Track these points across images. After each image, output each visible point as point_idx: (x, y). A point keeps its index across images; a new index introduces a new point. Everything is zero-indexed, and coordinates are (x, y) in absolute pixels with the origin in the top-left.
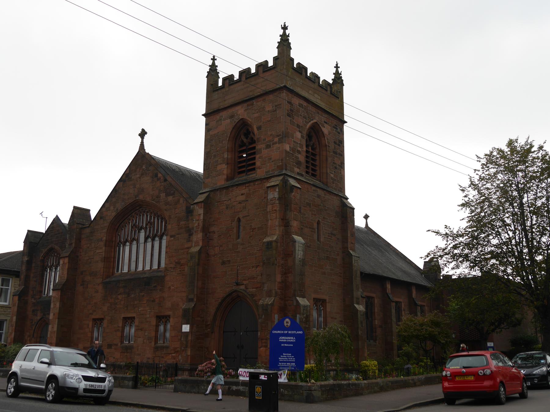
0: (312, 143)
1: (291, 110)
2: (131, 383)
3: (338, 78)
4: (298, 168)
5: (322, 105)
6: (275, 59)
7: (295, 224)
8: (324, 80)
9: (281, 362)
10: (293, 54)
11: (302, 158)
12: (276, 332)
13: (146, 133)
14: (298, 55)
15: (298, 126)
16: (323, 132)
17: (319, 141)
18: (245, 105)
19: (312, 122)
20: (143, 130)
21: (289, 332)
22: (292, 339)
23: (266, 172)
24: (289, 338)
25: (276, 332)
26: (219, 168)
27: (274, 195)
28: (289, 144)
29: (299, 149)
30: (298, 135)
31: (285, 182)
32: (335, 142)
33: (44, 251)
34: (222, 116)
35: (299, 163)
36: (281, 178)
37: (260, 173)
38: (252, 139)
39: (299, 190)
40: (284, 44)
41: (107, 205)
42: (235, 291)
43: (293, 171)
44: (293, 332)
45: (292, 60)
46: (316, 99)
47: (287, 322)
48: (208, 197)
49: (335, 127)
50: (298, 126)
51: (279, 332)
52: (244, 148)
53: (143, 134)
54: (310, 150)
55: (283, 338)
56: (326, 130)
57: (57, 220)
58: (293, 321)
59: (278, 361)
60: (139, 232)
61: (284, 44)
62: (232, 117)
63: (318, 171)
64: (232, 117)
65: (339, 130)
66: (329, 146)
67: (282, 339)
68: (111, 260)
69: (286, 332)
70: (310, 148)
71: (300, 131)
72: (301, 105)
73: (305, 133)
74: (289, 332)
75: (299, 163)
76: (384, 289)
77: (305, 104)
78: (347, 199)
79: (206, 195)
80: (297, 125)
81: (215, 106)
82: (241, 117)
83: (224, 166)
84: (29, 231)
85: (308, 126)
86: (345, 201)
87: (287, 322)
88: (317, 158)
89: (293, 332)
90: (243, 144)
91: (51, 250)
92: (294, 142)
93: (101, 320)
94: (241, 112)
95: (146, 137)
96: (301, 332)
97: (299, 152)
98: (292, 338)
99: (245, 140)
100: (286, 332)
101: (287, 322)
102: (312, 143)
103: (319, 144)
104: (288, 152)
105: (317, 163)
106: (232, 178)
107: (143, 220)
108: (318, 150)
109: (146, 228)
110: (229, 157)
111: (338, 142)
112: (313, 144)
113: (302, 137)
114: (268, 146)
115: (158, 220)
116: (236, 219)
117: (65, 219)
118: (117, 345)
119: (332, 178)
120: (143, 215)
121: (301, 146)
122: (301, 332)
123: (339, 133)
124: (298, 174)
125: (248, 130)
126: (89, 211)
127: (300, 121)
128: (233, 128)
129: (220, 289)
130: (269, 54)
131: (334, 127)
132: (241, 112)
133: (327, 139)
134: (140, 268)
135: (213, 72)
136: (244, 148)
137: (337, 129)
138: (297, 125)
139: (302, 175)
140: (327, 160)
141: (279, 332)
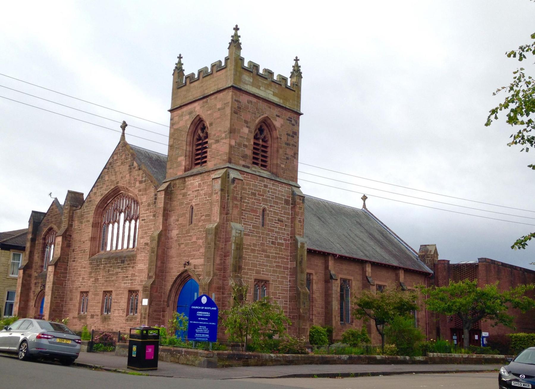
0: (262, 136)
1: (239, 108)
2: (86, 347)
3: (297, 72)
4: (244, 161)
5: (276, 100)
6: (227, 59)
7: (235, 212)
8: (279, 75)
9: (198, 333)
10: (243, 54)
11: (249, 152)
12: (194, 307)
13: (126, 125)
14: (248, 55)
15: (246, 122)
16: (274, 126)
17: (271, 134)
18: (201, 102)
19: (263, 116)
20: (124, 122)
21: (206, 308)
22: (207, 314)
23: (215, 165)
24: (205, 313)
25: (194, 307)
26: (180, 159)
27: (218, 185)
28: (234, 139)
29: (246, 143)
30: (246, 130)
31: (227, 175)
32: (287, 134)
33: (45, 230)
34: (183, 112)
35: (245, 157)
36: (223, 171)
37: (210, 165)
38: (207, 133)
39: (240, 182)
40: (235, 43)
41: (95, 190)
42: (186, 271)
43: (238, 164)
44: (209, 308)
45: (242, 60)
46: (269, 94)
47: (204, 300)
48: (168, 187)
49: (290, 120)
50: (246, 122)
51: (197, 307)
52: (200, 142)
53: (124, 126)
54: (261, 142)
55: (200, 313)
56: (278, 123)
57: (56, 202)
58: (209, 299)
59: (195, 333)
60: (119, 215)
61: (235, 43)
62: (190, 113)
63: (269, 162)
64: (190, 113)
65: (293, 122)
66: (281, 139)
67: (199, 313)
68: (99, 239)
69: (203, 308)
70: (261, 140)
71: (247, 127)
72: (249, 102)
73: (253, 128)
74: (206, 308)
75: (245, 157)
76: (364, 272)
77: (254, 100)
78: (299, 187)
79: (167, 184)
80: (245, 121)
81: (179, 103)
82: (198, 114)
83: (183, 158)
84: (33, 212)
85: (257, 121)
86: (295, 189)
87: (204, 300)
88: (269, 150)
89: (209, 308)
90: (199, 139)
91: (51, 229)
92: (241, 137)
93: (87, 292)
94: (197, 108)
95: (127, 128)
96: (215, 309)
97: (245, 146)
98: (207, 313)
99: (201, 135)
100: (203, 308)
101: (204, 300)
102: (262, 136)
103: (271, 137)
104: (234, 147)
105: (268, 154)
106: (191, 169)
107: (124, 203)
108: (269, 142)
109: (125, 211)
110: (188, 150)
111: (291, 134)
112: (265, 137)
113: (250, 131)
114: (217, 141)
115: (134, 204)
116: (190, 206)
117: (62, 202)
118: (97, 315)
119: (282, 169)
120: (123, 199)
121: (248, 140)
122: (215, 309)
123: (293, 125)
124: (244, 166)
125: (204, 125)
126: (82, 194)
127: (249, 117)
128: (192, 124)
129: (175, 269)
130: (221, 54)
131: (288, 120)
132: (197, 108)
133: (279, 132)
134: (120, 247)
135: (179, 70)
136: (200, 142)
137: (291, 121)
138: (245, 121)
139: (248, 167)
140: (278, 151)
141: (197, 307)
